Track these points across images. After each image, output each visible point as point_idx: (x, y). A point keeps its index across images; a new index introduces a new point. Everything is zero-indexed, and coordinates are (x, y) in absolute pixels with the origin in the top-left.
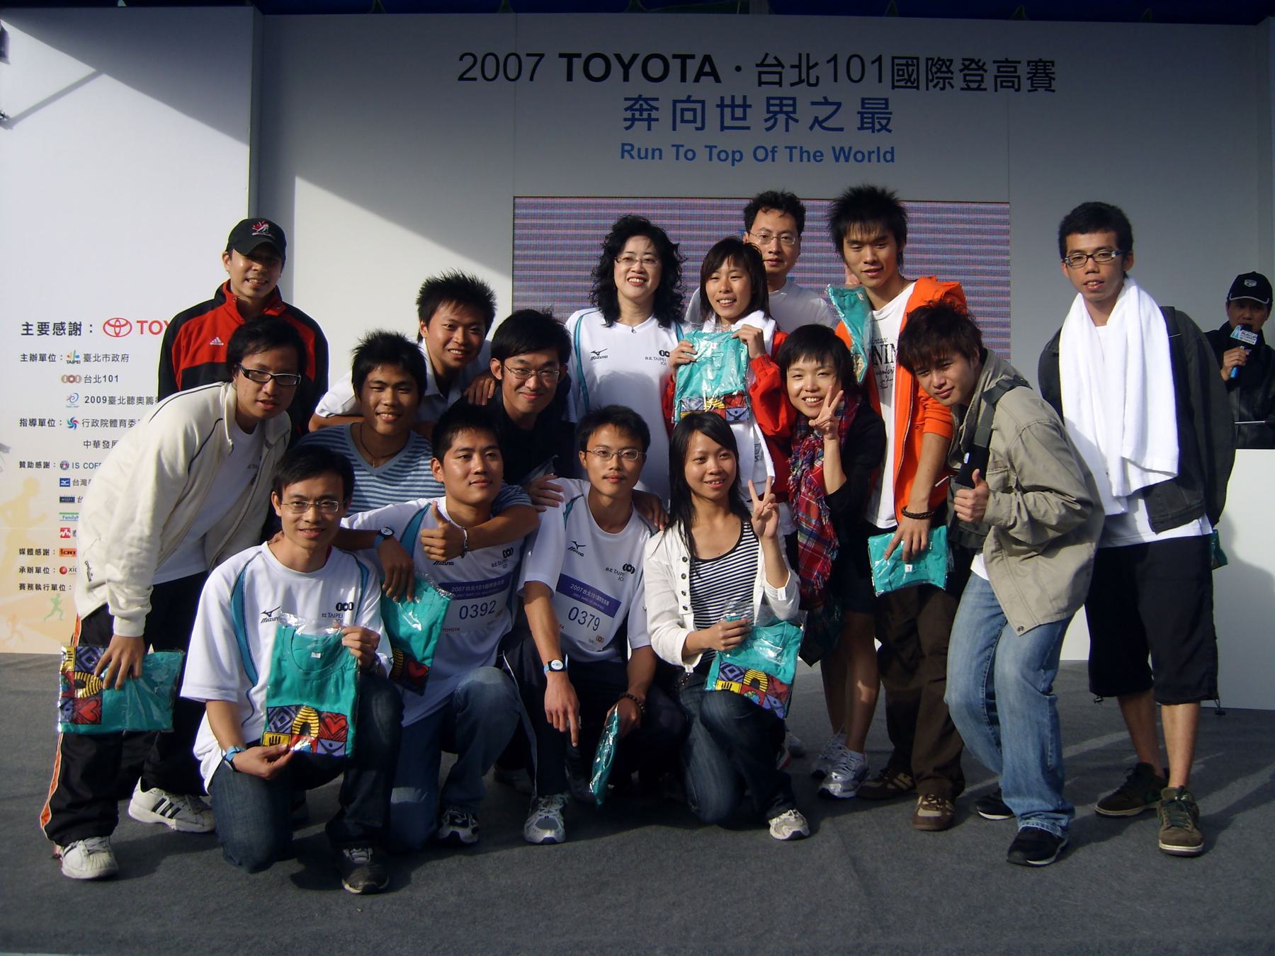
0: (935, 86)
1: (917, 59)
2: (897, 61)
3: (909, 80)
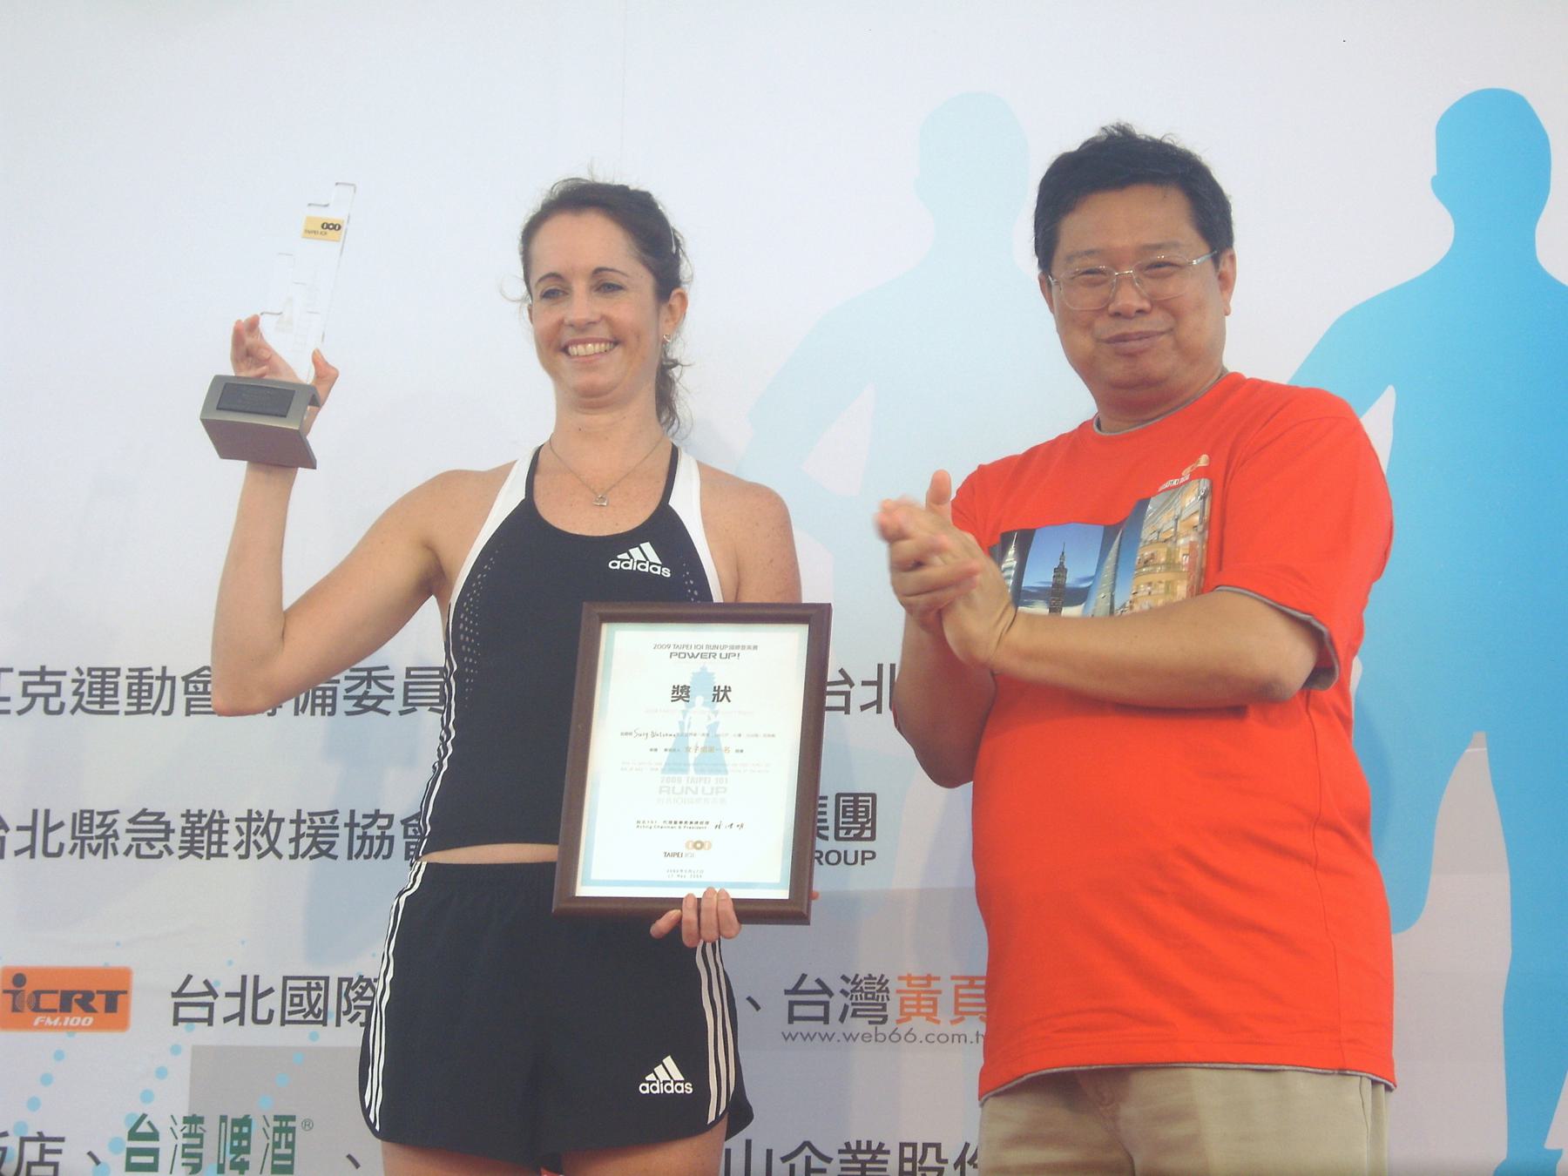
0: (351, 1020)
1: (327, 979)
2: (290, 983)
3: (311, 1011)
